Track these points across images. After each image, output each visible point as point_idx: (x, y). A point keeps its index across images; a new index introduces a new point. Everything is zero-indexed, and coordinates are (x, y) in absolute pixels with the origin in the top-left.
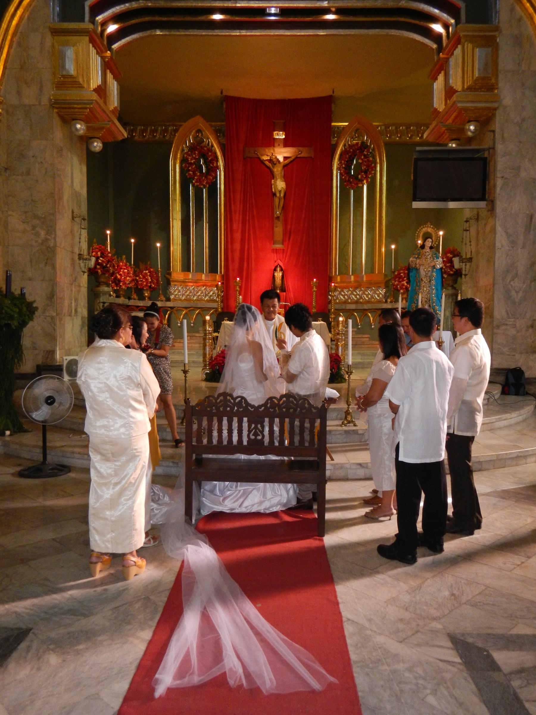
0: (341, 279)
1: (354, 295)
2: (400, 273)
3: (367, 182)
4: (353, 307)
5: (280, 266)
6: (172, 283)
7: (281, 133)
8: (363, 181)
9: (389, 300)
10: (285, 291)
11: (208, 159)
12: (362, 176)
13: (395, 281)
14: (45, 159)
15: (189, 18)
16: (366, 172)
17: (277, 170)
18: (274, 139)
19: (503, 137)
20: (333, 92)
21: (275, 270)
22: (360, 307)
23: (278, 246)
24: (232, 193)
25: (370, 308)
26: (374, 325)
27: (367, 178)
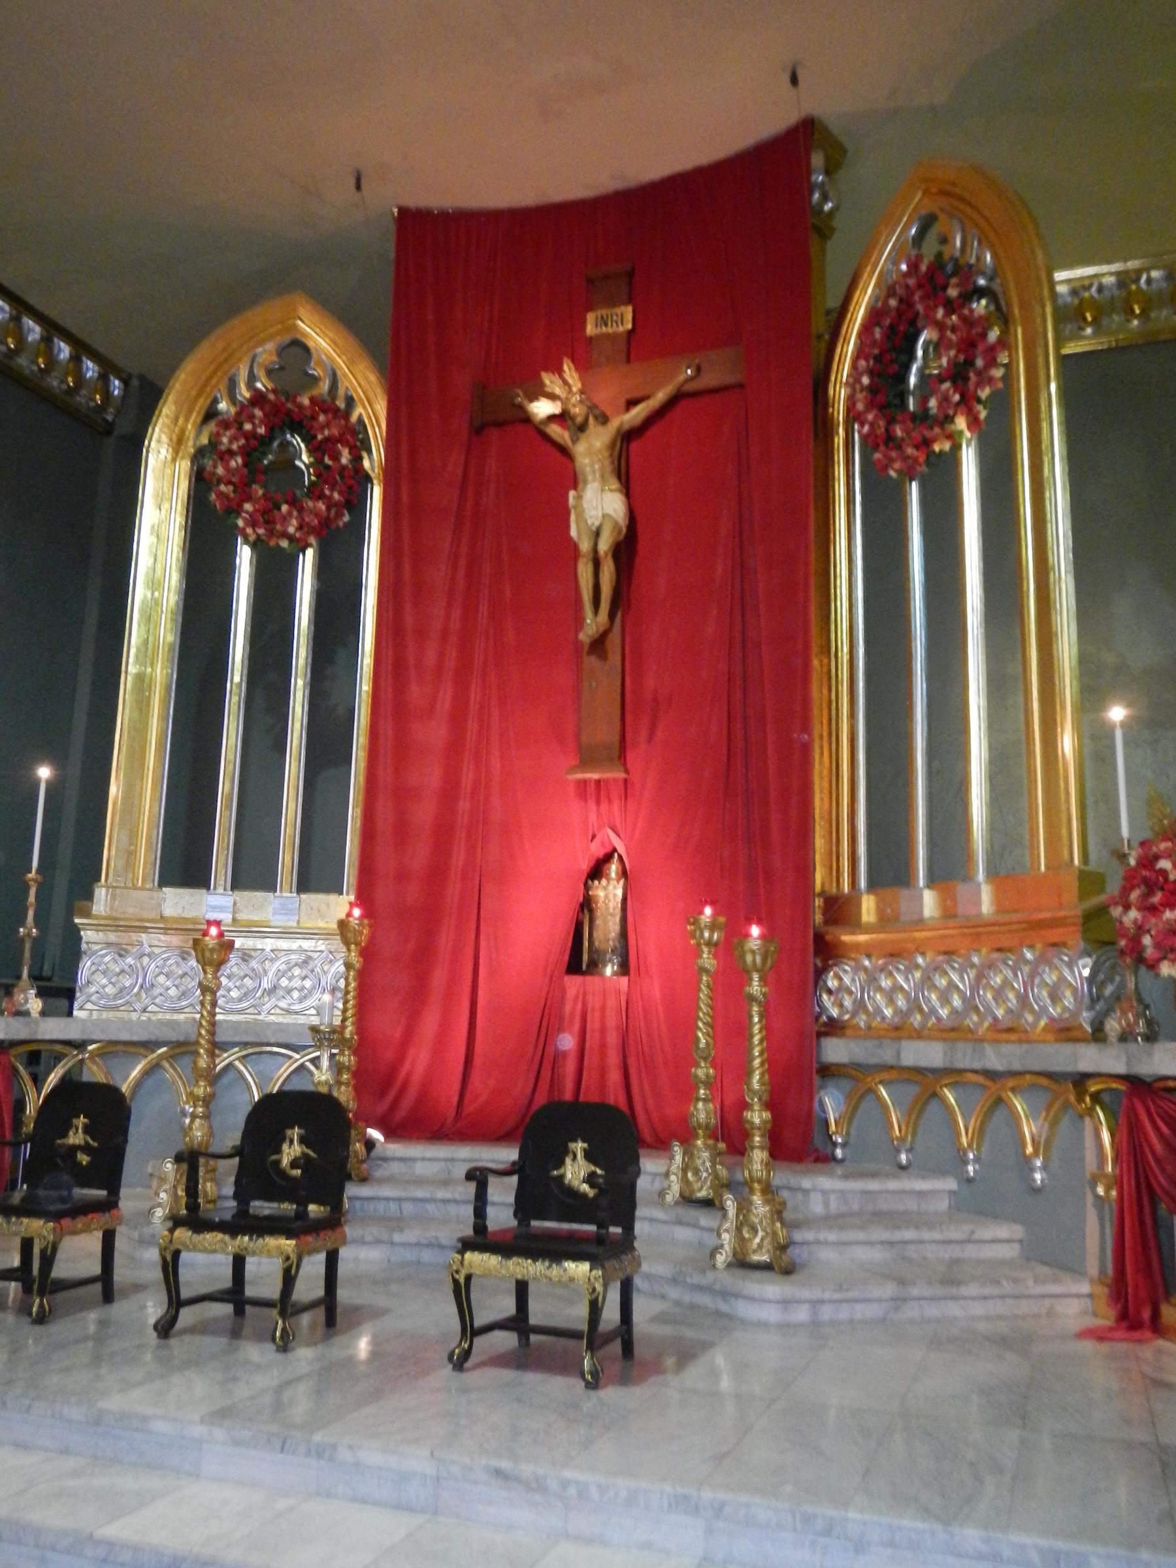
0: (880, 912)
3: (974, 423)
4: (931, 1054)
5: (620, 857)
8: (950, 419)
9: (1113, 1026)
11: (315, 437)
12: (945, 399)
17: (589, 453)
20: (794, 80)
21: (597, 872)
22: (965, 1057)
25: (1017, 1066)
27: (967, 402)
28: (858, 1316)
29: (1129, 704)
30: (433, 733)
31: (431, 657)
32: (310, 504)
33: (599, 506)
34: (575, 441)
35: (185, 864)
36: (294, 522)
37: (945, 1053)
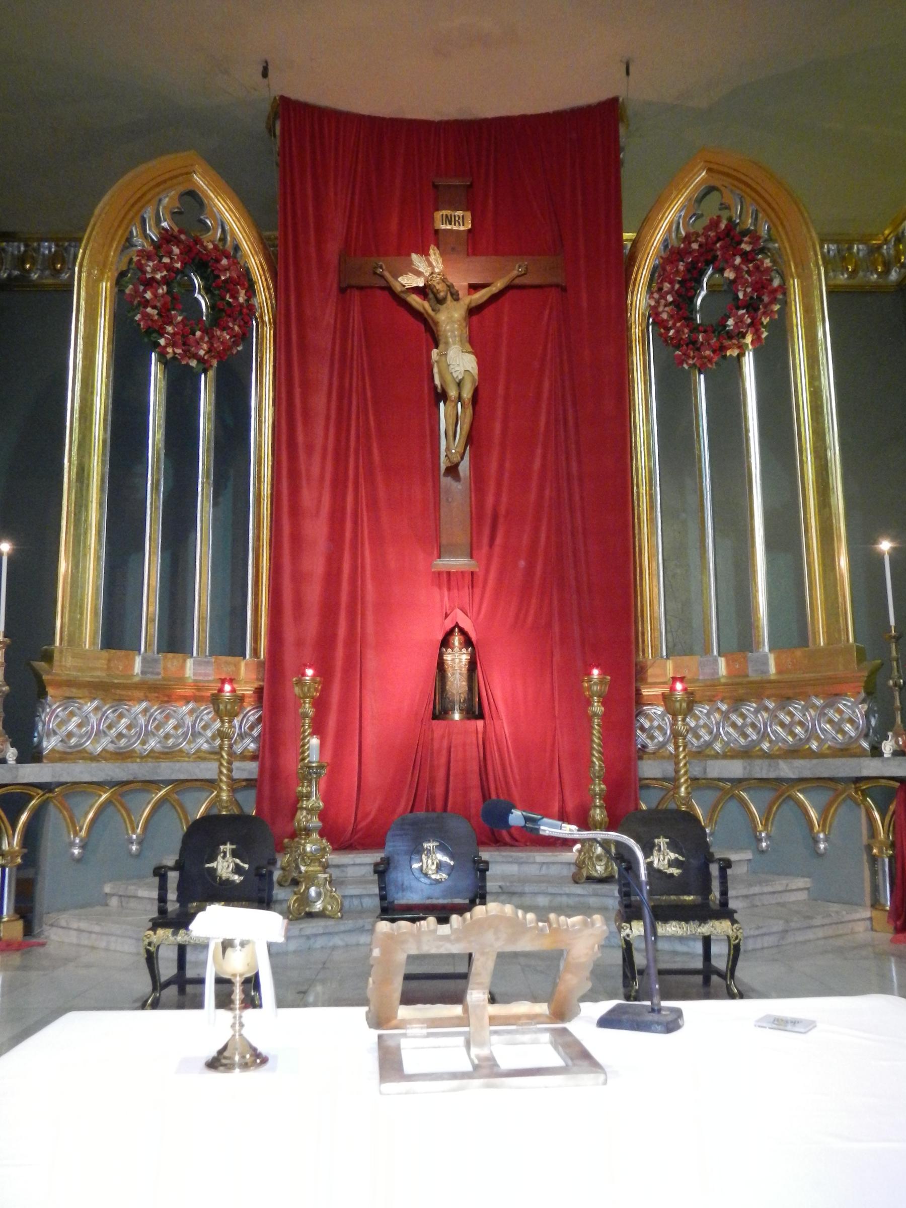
1: (734, 725)
3: (757, 339)
4: (735, 769)
6: (50, 691)
7: (460, 213)
8: (744, 336)
9: (888, 747)
10: (481, 716)
11: (219, 277)
12: (739, 321)
16: (752, 306)
17: (450, 319)
18: (437, 232)
21: (445, 643)
22: (761, 770)
23: (458, 563)
24: (297, 391)
25: (807, 774)
26: (826, 840)
27: (755, 325)
28: (766, 945)
29: (893, 539)
30: (317, 530)
31: (316, 470)
32: (219, 333)
33: (458, 363)
35: (117, 632)
36: (205, 346)
37: (745, 768)
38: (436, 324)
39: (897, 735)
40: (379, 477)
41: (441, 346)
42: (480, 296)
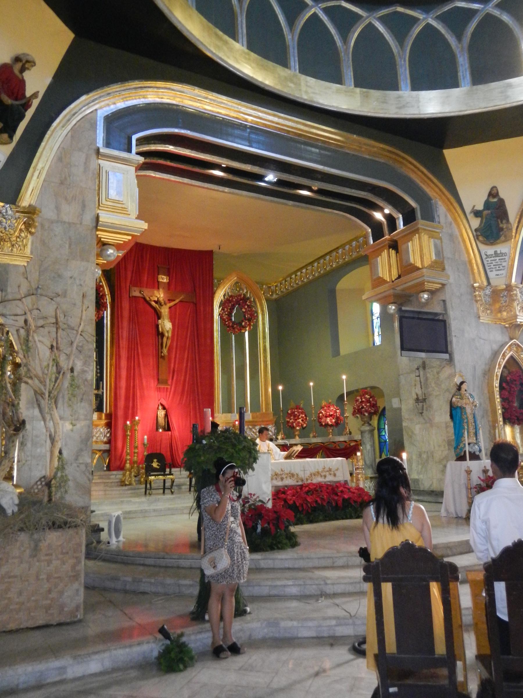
2: (295, 412)
3: (250, 328)
5: (162, 405)
9: (279, 437)
12: (246, 323)
13: (291, 419)
14: (84, 282)
15: (197, 170)
16: (249, 320)
18: (158, 282)
19: (452, 307)
33: (166, 325)
34: (161, 308)
38: (161, 312)
39: (282, 434)
40: (140, 357)
41: (162, 319)
42: (172, 304)
